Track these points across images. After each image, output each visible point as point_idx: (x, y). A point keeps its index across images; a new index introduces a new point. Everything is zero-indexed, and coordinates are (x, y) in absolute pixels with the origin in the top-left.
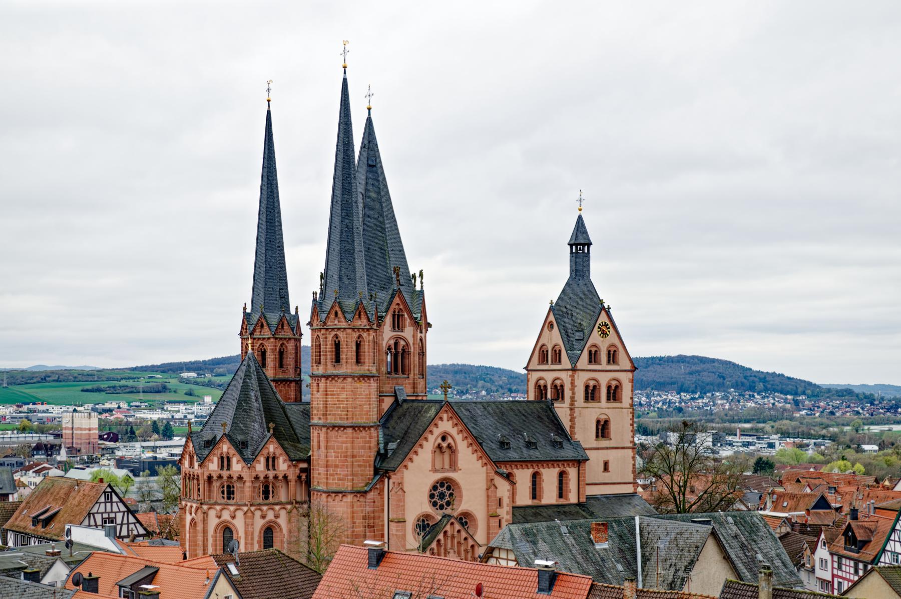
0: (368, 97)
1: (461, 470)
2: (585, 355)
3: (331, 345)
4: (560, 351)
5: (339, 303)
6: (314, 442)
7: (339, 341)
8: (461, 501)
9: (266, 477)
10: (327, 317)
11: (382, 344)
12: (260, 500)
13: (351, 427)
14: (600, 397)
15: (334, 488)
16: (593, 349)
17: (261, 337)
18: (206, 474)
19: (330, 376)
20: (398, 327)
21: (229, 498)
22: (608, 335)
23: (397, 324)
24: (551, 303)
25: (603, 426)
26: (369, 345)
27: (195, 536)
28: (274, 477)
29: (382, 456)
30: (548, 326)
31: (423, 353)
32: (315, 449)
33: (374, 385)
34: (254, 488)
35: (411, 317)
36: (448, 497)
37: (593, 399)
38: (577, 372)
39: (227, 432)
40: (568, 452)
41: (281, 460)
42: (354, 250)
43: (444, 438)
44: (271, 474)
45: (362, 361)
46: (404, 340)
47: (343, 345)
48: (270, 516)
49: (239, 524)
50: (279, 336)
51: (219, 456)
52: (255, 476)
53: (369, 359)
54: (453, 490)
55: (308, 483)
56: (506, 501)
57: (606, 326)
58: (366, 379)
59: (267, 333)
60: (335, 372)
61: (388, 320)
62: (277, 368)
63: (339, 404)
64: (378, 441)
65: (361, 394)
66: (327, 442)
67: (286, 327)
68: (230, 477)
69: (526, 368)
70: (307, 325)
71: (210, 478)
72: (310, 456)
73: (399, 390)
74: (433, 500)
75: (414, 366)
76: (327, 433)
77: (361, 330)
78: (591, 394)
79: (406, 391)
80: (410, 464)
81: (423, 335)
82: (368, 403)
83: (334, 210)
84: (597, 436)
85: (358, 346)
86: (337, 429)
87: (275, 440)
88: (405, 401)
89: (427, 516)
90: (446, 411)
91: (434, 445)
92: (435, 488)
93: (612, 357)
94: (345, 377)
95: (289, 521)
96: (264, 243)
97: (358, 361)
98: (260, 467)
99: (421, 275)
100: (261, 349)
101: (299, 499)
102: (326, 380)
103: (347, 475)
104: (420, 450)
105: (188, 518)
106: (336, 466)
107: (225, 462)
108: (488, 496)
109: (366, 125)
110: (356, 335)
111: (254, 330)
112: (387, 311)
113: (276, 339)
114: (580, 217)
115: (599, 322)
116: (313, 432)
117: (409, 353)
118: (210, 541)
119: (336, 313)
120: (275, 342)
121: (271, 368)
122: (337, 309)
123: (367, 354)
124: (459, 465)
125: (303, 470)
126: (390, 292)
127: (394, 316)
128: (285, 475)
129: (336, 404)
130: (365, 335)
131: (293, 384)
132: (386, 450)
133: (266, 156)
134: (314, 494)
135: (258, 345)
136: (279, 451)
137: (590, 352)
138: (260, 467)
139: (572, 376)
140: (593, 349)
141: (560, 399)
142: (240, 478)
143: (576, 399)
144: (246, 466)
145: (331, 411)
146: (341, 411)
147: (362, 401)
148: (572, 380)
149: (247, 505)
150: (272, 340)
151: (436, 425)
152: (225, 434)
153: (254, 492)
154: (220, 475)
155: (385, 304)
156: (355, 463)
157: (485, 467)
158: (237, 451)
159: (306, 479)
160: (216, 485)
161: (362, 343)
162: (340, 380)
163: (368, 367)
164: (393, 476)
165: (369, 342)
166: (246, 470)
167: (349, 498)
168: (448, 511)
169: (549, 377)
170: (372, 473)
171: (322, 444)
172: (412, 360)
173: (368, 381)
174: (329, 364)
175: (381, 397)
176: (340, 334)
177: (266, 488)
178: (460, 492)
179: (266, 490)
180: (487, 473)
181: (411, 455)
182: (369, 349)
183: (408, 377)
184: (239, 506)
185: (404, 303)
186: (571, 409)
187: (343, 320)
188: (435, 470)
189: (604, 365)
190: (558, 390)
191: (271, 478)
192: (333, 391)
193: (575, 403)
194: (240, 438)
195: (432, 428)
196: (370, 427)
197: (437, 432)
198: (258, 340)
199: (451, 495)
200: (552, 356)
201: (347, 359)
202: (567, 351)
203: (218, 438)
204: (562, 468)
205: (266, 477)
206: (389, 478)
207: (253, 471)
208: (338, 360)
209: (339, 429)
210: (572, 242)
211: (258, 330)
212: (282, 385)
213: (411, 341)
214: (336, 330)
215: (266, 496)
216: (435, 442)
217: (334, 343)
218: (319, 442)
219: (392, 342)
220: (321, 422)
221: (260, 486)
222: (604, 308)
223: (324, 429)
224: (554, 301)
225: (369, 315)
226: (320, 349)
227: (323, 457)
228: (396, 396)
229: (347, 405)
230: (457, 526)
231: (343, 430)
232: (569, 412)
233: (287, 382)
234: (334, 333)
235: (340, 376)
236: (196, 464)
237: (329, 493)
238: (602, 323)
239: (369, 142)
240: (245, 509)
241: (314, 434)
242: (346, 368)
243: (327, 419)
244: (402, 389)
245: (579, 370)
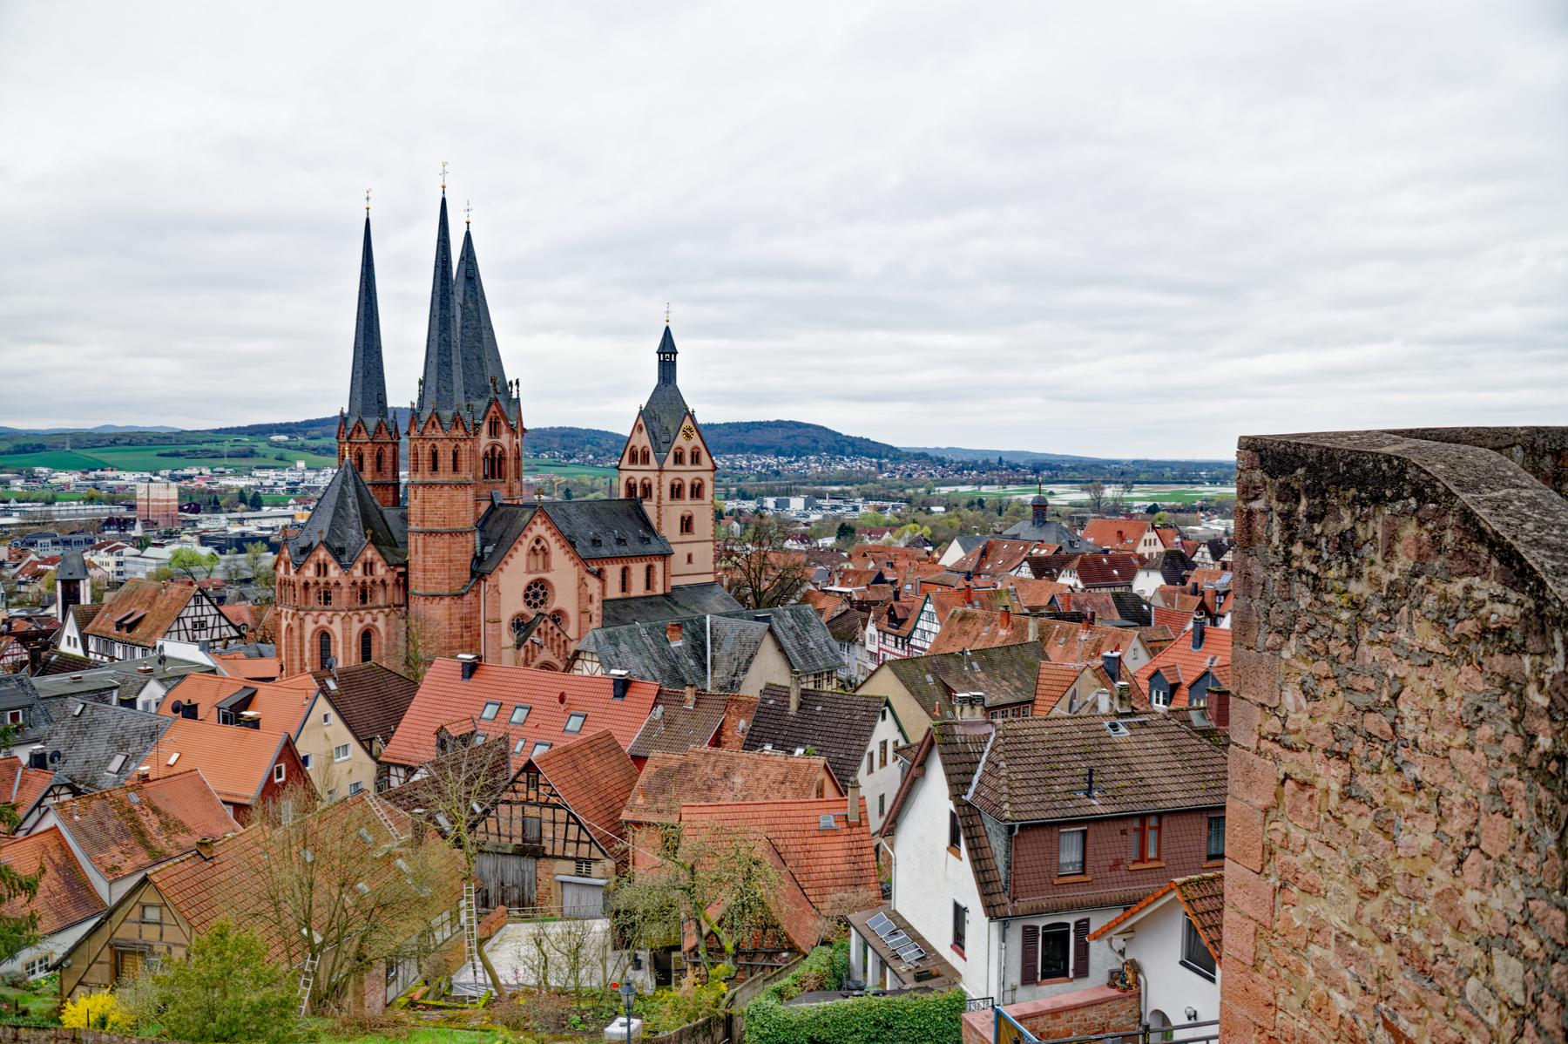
2: (671, 457)
6: (412, 547)
9: (364, 582)
10: (425, 428)
12: (358, 605)
15: (432, 591)
18: (303, 580)
21: (326, 604)
23: (494, 431)
27: (292, 642)
29: (478, 559)
33: (471, 491)
35: (508, 425)
37: (678, 497)
40: (655, 547)
43: (538, 542)
44: (369, 579)
47: (441, 454)
48: (368, 620)
49: (336, 629)
55: (406, 586)
56: (597, 597)
59: (364, 437)
60: (433, 480)
61: (485, 427)
67: (384, 431)
68: (327, 583)
71: (306, 585)
78: (676, 492)
79: (501, 496)
80: (505, 567)
85: (455, 455)
88: (501, 505)
89: (522, 615)
92: (529, 588)
93: (696, 458)
94: (442, 485)
95: (387, 625)
97: (455, 468)
98: (358, 572)
99: (517, 383)
101: (396, 602)
105: (284, 624)
106: (434, 571)
107: (322, 569)
111: (352, 434)
112: (484, 419)
114: (667, 328)
118: (307, 646)
122: (434, 419)
125: (400, 574)
127: (490, 423)
130: (462, 444)
136: (377, 557)
137: (676, 454)
138: (358, 572)
139: (659, 476)
142: (337, 584)
155: (482, 412)
159: (403, 582)
160: (313, 591)
167: (447, 601)
168: (541, 609)
171: (420, 550)
175: (477, 503)
178: (553, 591)
179: (364, 594)
181: (506, 559)
184: (336, 612)
185: (501, 411)
188: (529, 572)
189: (688, 465)
191: (369, 583)
194: (337, 544)
196: (467, 533)
197: (531, 536)
199: (545, 594)
205: (364, 582)
208: (435, 468)
211: (355, 434)
213: (507, 448)
219: (489, 448)
220: (419, 528)
223: (422, 536)
227: (420, 562)
228: (492, 500)
230: (550, 624)
233: (384, 485)
234: (431, 443)
237: (426, 597)
240: (343, 614)
241: (411, 539)
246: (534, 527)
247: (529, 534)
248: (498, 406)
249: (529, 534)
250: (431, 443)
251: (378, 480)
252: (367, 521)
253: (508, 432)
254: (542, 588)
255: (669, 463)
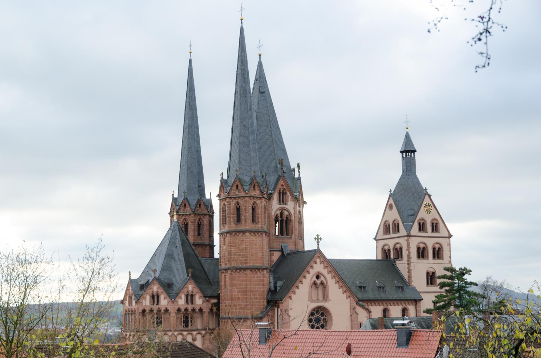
0: (259, 48)
1: (331, 300)
2: (416, 226)
3: (234, 209)
4: (398, 224)
5: (239, 179)
6: (222, 283)
7: (240, 207)
8: (331, 325)
9: (186, 310)
11: (271, 213)
13: (249, 269)
14: (428, 256)
16: (422, 222)
17: (184, 213)
19: (233, 232)
20: (283, 202)
22: (431, 212)
23: (282, 199)
24: (391, 191)
25: (431, 276)
26: (262, 209)
28: (192, 310)
29: (273, 292)
30: (389, 208)
31: (301, 222)
32: (223, 288)
33: (265, 239)
34: (177, 318)
35: (292, 195)
36: (322, 321)
37: (423, 257)
38: (411, 237)
39: (157, 276)
40: (408, 295)
41: (197, 297)
42: (249, 142)
43: (318, 277)
44: (190, 307)
45: (256, 221)
46: (287, 211)
47: (243, 209)
50: (198, 213)
51: (151, 294)
52: (177, 308)
53: (262, 219)
54: (326, 316)
55: (218, 315)
57: (430, 206)
58: (260, 234)
59: (188, 211)
61: (276, 196)
62: (196, 236)
63: (240, 252)
64: (270, 281)
65: (256, 245)
66: (232, 281)
67: (202, 206)
68: (159, 311)
69: (375, 239)
70: (217, 196)
72: (219, 294)
73: (284, 246)
74: (311, 324)
75: (295, 230)
76: (231, 274)
77: (255, 198)
78: (422, 253)
79: (289, 247)
81: (301, 209)
82: (261, 252)
83: (235, 115)
84: (428, 284)
85: (253, 209)
86: (238, 271)
87: (192, 282)
88: (289, 254)
90: (318, 256)
91: (311, 281)
92: (312, 314)
93: (435, 227)
94: (244, 232)
96: (186, 148)
97: (253, 220)
98: (181, 302)
99: (298, 166)
100: (185, 223)
102: (231, 234)
103: (247, 305)
104: (300, 285)
107: (155, 298)
108: (352, 321)
109: (258, 66)
110: (252, 202)
111: (179, 209)
112: (274, 189)
113: (195, 214)
114: (407, 134)
115: (425, 203)
116: (221, 275)
117: (291, 221)
119: (237, 186)
120: (195, 217)
121: (192, 236)
122: (238, 183)
123: (260, 216)
124: (329, 297)
126: (277, 177)
127: (279, 193)
128: (200, 308)
129: (238, 253)
130: (258, 202)
131: (208, 248)
132: (275, 287)
133: (188, 89)
134: (222, 322)
135: (182, 220)
136: (196, 290)
137: (419, 223)
139: (408, 240)
140: (422, 222)
141: (400, 258)
142: (166, 310)
143: (411, 257)
144: (171, 301)
145: (234, 258)
146: (241, 257)
147: (257, 250)
148: (408, 243)
149: (171, 331)
150: (192, 215)
151: (312, 267)
152: (155, 277)
153: (177, 321)
154: (152, 309)
155: (273, 185)
156: (252, 296)
157: (349, 299)
158: (164, 290)
160: (148, 317)
161: (256, 208)
162: (240, 235)
163: (261, 225)
164: (281, 305)
165: (261, 207)
166: (170, 304)
169: (391, 244)
170: (265, 303)
172: (293, 225)
173: (261, 236)
174: (232, 223)
175: (271, 250)
176: (240, 201)
177: (186, 318)
178: (331, 317)
180: (350, 303)
182: (262, 212)
183: (291, 238)
185: (287, 185)
186: (408, 264)
187: (242, 191)
188: (312, 301)
189: (429, 233)
190: (398, 252)
191: (190, 310)
192: (236, 243)
193: (411, 259)
195: (309, 269)
196: (263, 269)
197: (313, 272)
198: (182, 217)
200: (393, 228)
201: (245, 219)
202: (403, 223)
203: (150, 282)
204: (404, 306)
205: (186, 310)
206: (278, 307)
207: (176, 304)
208: (239, 220)
209: (240, 271)
210: (403, 150)
211: (182, 209)
212: (199, 248)
213: (292, 212)
214: (237, 198)
215: (186, 324)
216: (311, 280)
217: (236, 208)
218: (225, 282)
219: (279, 212)
220: (228, 266)
221: (181, 316)
222: (427, 193)
223: (229, 272)
224: (393, 190)
225: (261, 188)
226: (226, 213)
228: (282, 251)
229: (246, 252)
231: (243, 272)
232: (406, 266)
233: (203, 245)
234: (236, 201)
235: (240, 231)
236: (134, 302)
238: (427, 203)
239: (260, 77)
240: (170, 333)
242: (245, 226)
243: (231, 264)
244: (287, 246)
245: (412, 236)
246: (315, 265)
247: (311, 270)
248: (285, 182)
249: (311, 270)
250: (235, 201)
251: (199, 241)
252: (189, 264)
253: (292, 200)
254: (322, 315)
255: (415, 230)
